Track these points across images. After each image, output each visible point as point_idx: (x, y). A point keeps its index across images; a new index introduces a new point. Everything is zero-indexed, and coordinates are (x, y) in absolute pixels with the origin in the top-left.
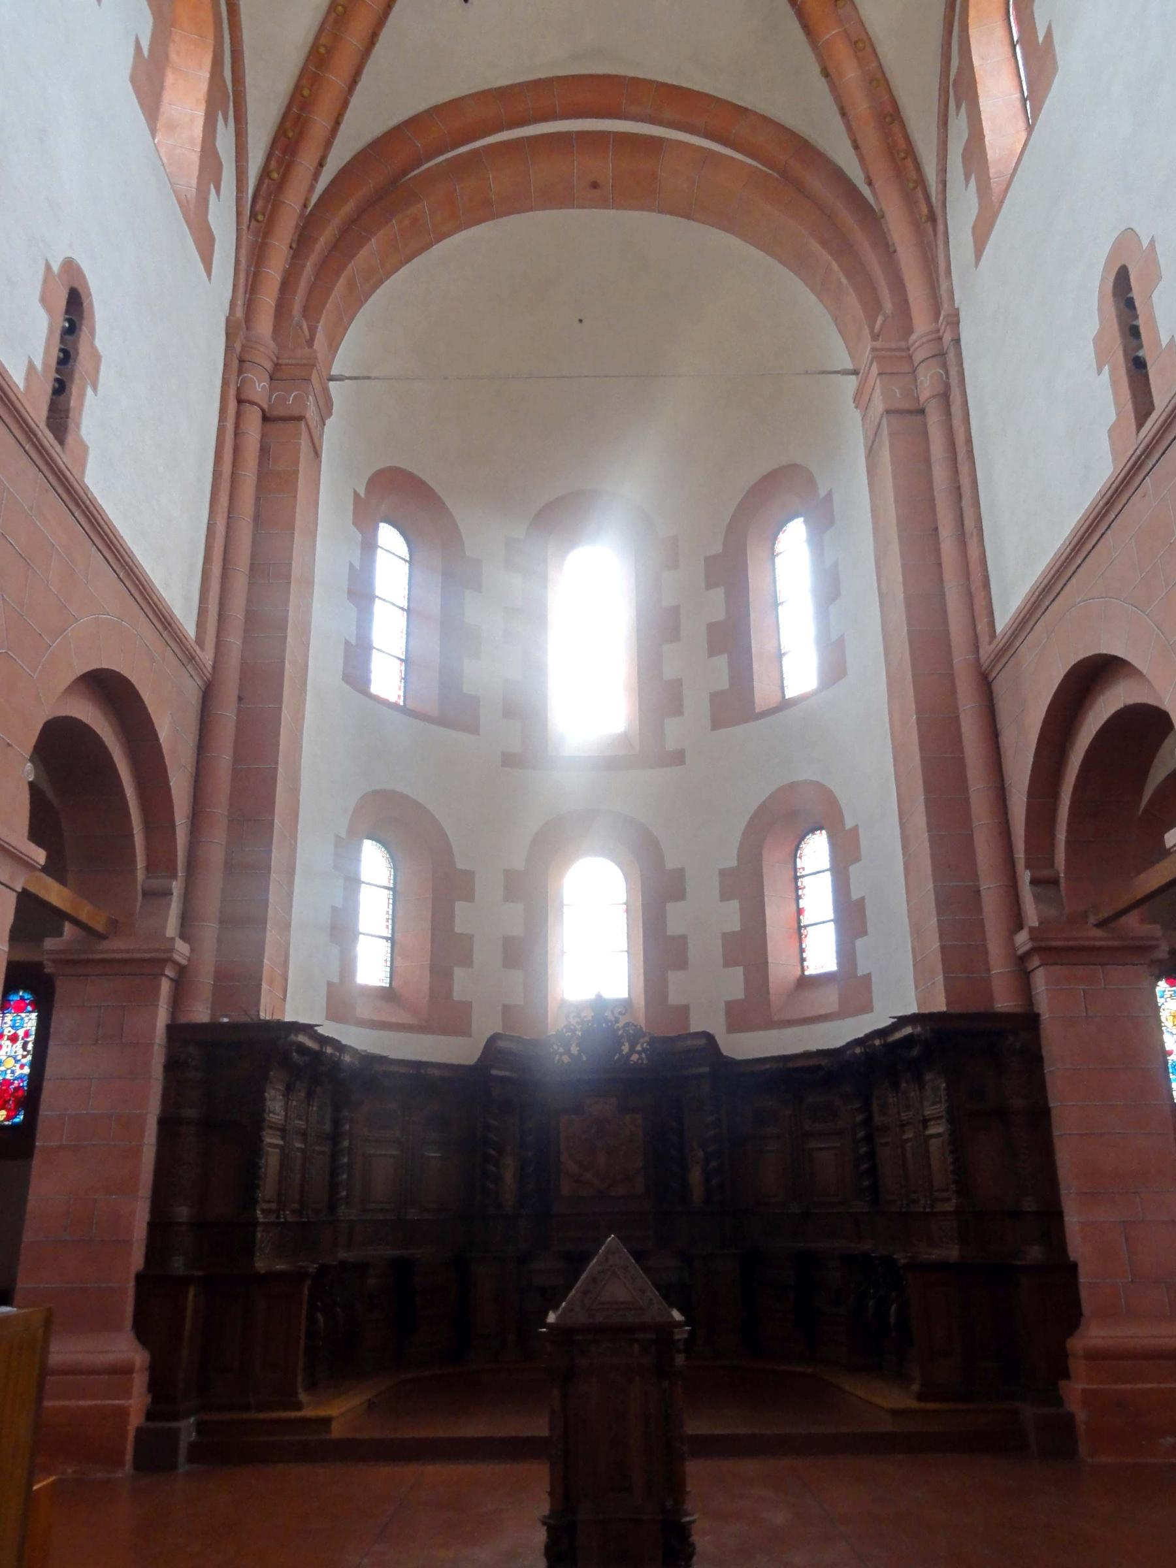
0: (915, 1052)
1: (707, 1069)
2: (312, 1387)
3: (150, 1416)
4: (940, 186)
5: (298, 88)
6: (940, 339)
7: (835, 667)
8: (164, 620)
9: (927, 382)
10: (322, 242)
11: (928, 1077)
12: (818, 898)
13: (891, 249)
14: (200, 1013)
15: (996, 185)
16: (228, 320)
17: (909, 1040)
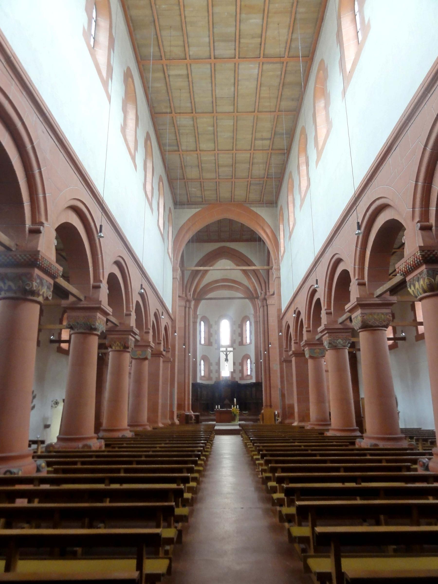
7: (251, 343)
9: (258, 320)
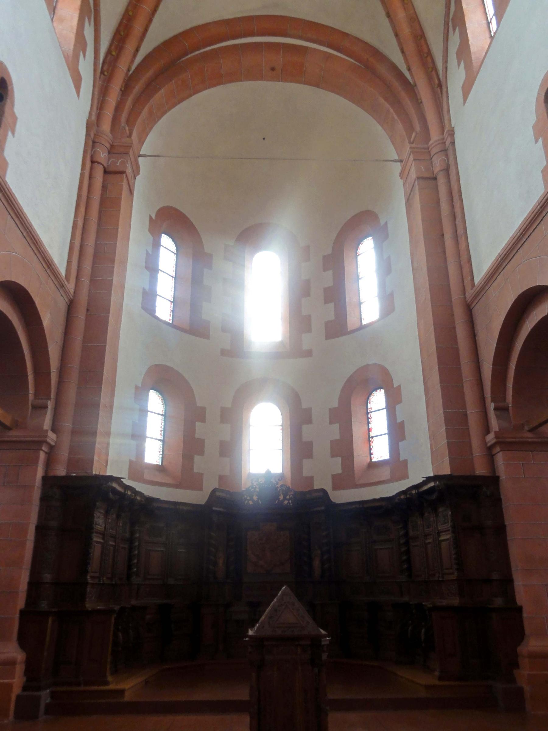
0: (434, 496)
1: (323, 508)
2: (115, 671)
3: (25, 688)
4: (444, 70)
5: (127, 11)
6: (445, 143)
8: (48, 264)
9: (438, 164)
10: (137, 88)
11: (441, 510)
12: (379, 423)
13: (419, 101)
14: (61, 471)
15: (475, 64)
16: (87, 121)
17: (432, 490)
